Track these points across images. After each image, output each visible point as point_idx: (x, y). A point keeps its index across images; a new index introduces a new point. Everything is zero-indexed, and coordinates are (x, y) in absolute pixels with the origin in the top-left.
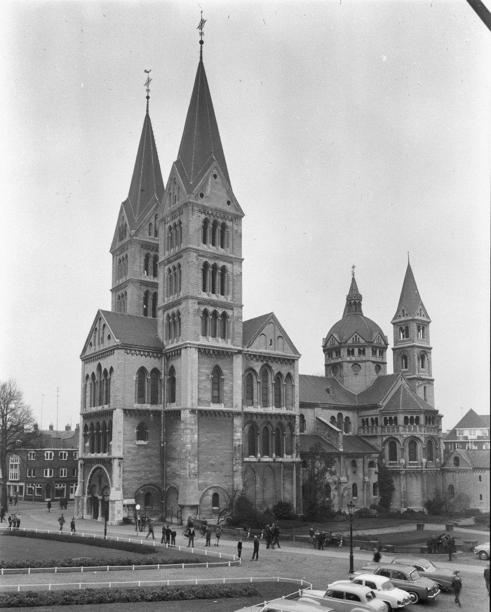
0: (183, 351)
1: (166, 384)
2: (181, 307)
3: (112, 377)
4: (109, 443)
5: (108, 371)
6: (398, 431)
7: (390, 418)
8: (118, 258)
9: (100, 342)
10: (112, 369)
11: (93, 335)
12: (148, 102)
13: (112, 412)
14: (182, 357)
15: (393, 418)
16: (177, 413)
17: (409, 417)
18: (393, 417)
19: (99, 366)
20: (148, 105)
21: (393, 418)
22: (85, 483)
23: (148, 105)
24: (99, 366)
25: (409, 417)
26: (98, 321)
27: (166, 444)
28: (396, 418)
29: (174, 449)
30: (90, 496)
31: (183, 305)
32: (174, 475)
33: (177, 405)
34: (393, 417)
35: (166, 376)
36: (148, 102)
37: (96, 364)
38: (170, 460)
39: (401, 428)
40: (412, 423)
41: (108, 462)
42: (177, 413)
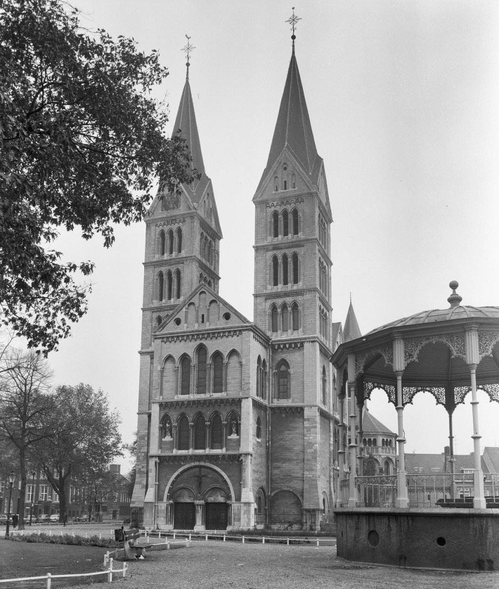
0: (306, 345)
1: (271, 377)
2: (299, 299)
3: (231, 361)
4: (226, 437)
5: (225, 354)
6: (377, 452)
7: (370, 440)
8: (159, 229)
9: (201, 320)
10: (233, 352)
11: (184, 310)
12: (188, 69)
13: (241, 402)
14: (305, 351)
15: (372, 440)
16: (298, 411)
17: (385, 439)
18: (372, 439)
19: (201, 350)
20: (188, 72)
21: (372, 440)
22: (162, 487)
23: (188, 72)
24: (201, 349)
25: (385, 439)
26: (198, 294)
27: (271, 444)
28: (375, 440)
29: (289, 449)
30: (171, 502)
31: (308, 296)
32: (289, 477)
33: (293, 402)
34: (372, 439)
35: (271, 370)
36: (188, 69)
37: (194, 344)
38: (278, 462)
39: (380, 449)
40: (370, 445)
41: (235, 462)
42: (298, 411)
